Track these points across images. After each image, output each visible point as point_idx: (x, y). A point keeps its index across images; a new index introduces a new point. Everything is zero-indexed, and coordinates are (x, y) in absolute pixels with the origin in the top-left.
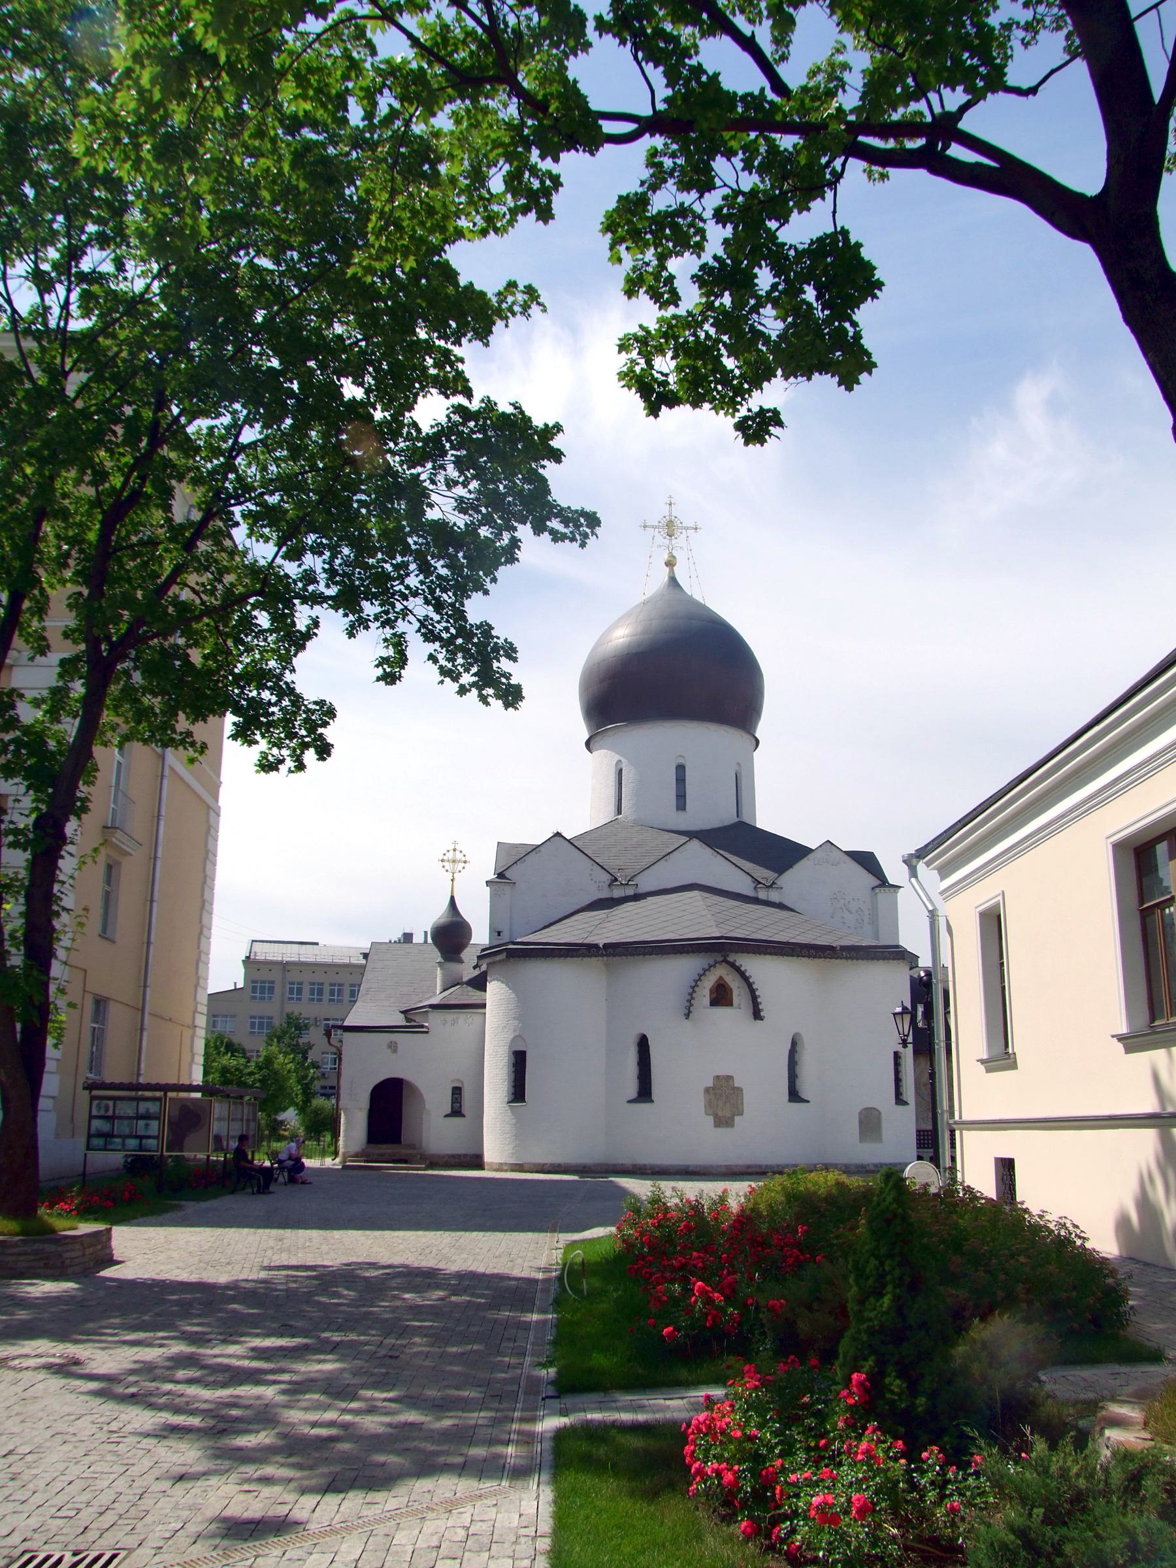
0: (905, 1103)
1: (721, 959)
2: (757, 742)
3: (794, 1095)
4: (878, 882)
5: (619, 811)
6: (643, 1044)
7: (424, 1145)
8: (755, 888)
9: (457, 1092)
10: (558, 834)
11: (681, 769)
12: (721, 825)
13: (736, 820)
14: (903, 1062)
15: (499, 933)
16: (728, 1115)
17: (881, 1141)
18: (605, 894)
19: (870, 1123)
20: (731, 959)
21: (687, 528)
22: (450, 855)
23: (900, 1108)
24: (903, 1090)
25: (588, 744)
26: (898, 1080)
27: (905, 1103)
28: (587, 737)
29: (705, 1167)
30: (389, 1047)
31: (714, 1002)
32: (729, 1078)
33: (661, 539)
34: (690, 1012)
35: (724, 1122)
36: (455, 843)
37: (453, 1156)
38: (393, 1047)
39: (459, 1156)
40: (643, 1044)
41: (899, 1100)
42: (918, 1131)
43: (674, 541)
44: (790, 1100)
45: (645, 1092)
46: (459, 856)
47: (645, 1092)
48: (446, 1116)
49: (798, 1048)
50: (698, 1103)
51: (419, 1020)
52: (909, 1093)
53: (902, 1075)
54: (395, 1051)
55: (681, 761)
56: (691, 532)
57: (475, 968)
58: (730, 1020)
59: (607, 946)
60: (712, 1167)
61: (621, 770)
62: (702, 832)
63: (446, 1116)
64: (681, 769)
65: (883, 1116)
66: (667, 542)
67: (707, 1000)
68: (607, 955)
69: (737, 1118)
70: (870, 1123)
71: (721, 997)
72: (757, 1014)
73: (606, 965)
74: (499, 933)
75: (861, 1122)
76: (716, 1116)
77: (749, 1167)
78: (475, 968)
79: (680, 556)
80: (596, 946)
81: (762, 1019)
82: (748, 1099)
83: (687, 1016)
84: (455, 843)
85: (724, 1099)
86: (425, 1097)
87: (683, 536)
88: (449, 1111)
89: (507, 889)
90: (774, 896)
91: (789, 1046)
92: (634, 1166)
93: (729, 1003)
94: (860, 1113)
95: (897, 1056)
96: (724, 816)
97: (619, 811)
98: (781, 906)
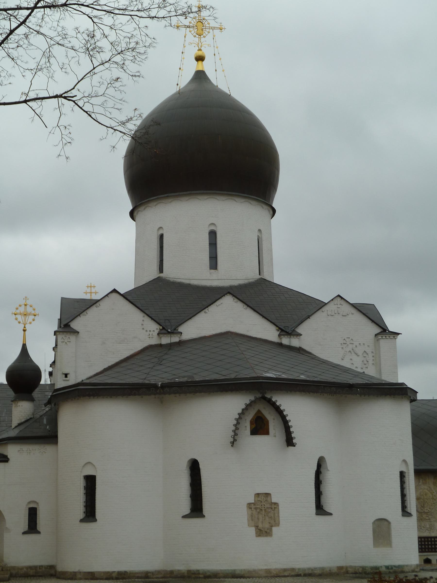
0: (410, 515)
1: (260, 396)
2: (274, 211)
3: (320, 509)
4: (378, 330)
5: (161, 270)
6: (194, 467)
7: (5, 559)
8: (279, 335)
9: (33, 513)
10: (115, 291)
11: (213, 235)
12: (246, 282)
13: (258, 277)
14: (406, 479)
15: (66, 375)
16: (267, 526)
17: (391, 546)
18: (154, 341)
19: (382, 530)
20: (268, 396)
21: (213, 28)
22: (22, 309)
23: (406, 519)
24: (408, 504)
25: (132, 214)
26: (403, 496)
27: (410, 515)
28: (131, 208)
29: (249, 572)
31: (254, 432)
32: (268, 495)
33: (191, 38)
34: (235, 440)
35: (263, 532)
37: (30, 568)
39: (35, 567)
40: (194, 467)
41: (405, 512)
42: (419, 538)
43: (203, 39)
44: (317, 514)
45: (197, 508)
46: (29, 310)
47: (197, 508)
48: (24, 533)
49: (322, 470)
50: (243, 515)
52: (412, 507)
53: (407, 491)
55: (212, 228)
56: (217, 32)
57: (46, 405)
58: (266, 445)
59: (164, 386)
60: (254, 571)
61: (161, 237)
62: (231, 287)
63: (24, 533)
64: (213, 235)
65: (393, 526)
66: (197, 39)
67: (248, 431)
68: (165, 393)
69: (274, 529)
70: (382, 530)
71: (259, 427)
72: (290, 441)
73: (162, 402)
74: (66, 375)
75: (374, 531)
76: (257, 527)
77: (285, 570)
78: (46, 405)
79: (207, 52)
80: (155, 386)
81: (293, 445)
82: (284, 513)
83: (233, 443)
85: (264, 513)
86: (6, 518)
87: (210, 36)
88: (26, 528)
89: (73, 338)
90: (295, 342)
91: (315, 468)
92: (189, 571)
93: (267, 433)
94: (374, 523)
95: (402, 475)
96: (249, 274)
97: (161, 270)
98: (300, 350)
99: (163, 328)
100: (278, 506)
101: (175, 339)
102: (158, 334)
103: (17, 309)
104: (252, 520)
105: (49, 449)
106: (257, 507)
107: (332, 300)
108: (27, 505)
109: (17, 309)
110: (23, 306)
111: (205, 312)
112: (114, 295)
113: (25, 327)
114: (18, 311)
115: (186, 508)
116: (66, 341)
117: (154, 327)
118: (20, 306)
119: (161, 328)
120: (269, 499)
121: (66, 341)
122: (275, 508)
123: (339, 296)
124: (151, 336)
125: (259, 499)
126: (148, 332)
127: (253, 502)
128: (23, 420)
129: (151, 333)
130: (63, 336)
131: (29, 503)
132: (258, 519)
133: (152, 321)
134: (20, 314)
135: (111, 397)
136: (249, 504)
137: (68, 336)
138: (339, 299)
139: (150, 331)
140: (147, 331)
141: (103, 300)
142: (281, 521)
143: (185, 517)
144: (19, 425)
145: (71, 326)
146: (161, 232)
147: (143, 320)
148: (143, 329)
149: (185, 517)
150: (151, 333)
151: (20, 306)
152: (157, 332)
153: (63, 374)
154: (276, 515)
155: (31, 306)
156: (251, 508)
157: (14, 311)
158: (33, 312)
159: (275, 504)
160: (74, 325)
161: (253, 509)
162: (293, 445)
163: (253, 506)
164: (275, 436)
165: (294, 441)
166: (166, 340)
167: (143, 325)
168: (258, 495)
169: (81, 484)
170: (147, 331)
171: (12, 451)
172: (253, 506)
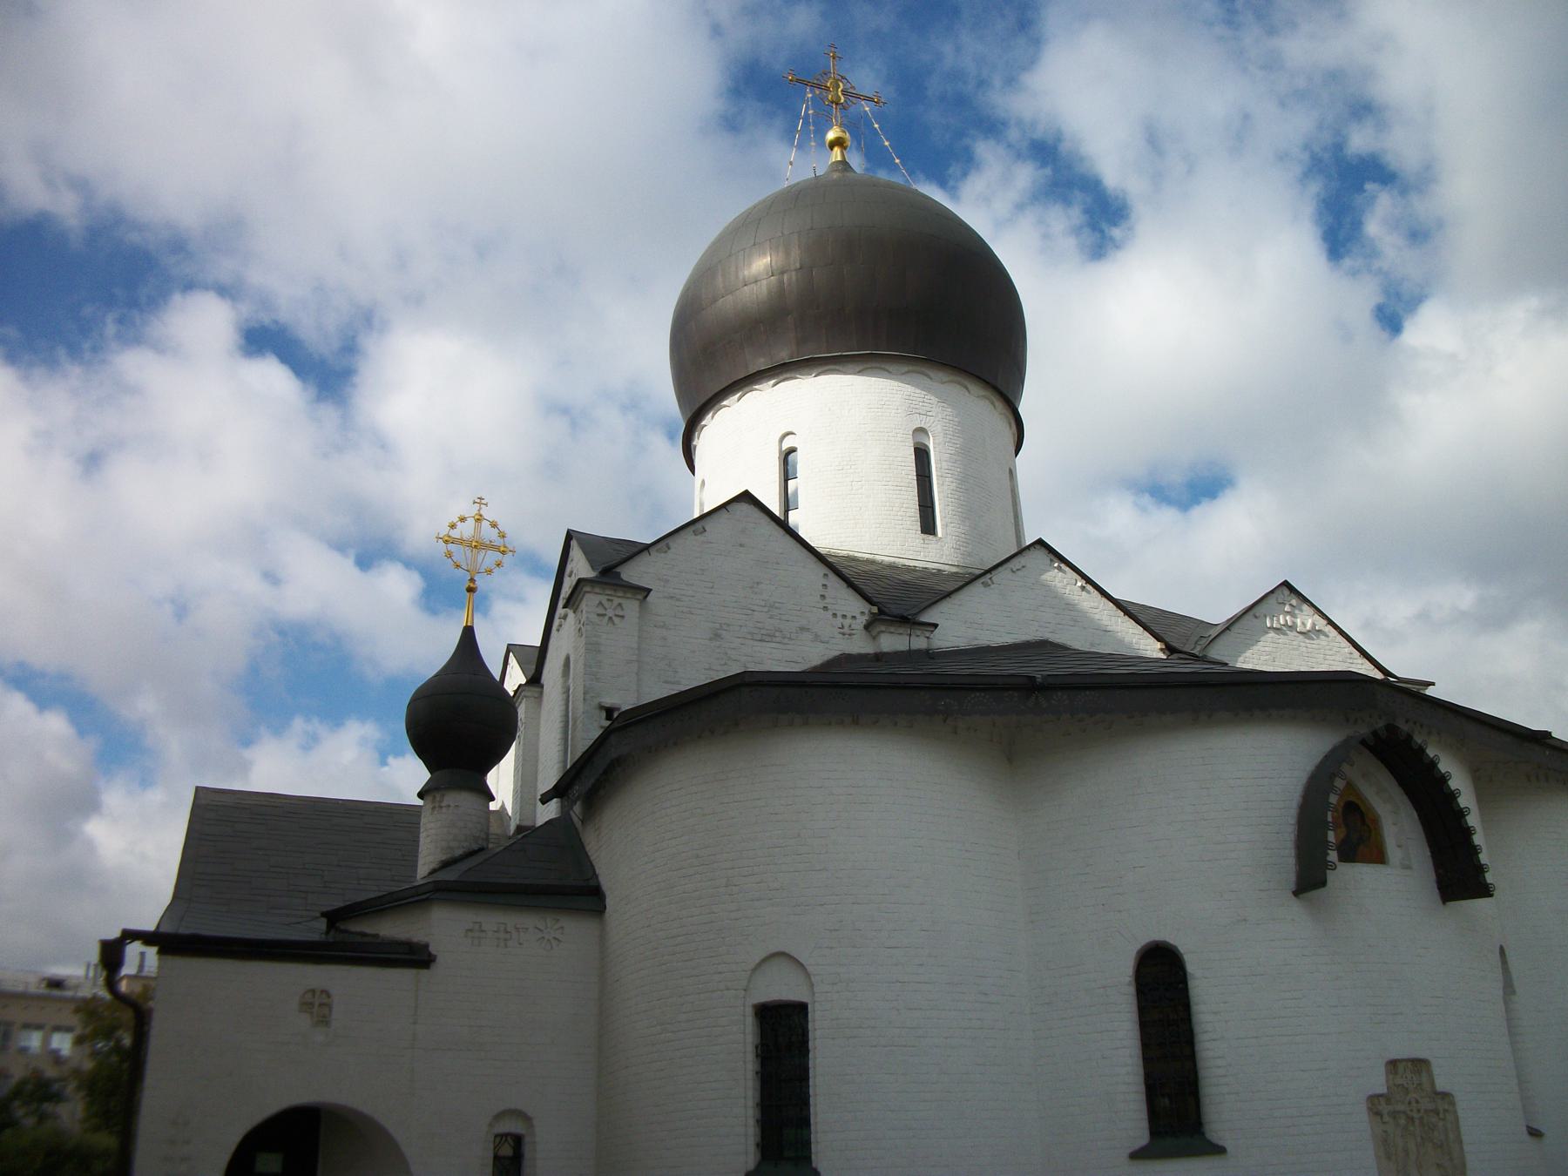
6: (1161, 978)
18: (860, 645)
22: (466, 530)
30: (306, 1006)
31: (1350, 854)
36: (480, 501)
38: (318, 1006)
40: (1161, 978)
46: (489, 534)
51: (391, 928)
54: (324, 1021)
73: (1010, 760)
78: (545, 799)
84: (480, 501)
89: (631, 606)
93: (1379, 857)
99: (881, 612)
100: (1453, 1104)
101: (919, 643)
102: (867, 627)
103: (453, 526)
104: (1389, 1158)
105: (572, 932)
106: (1401, 1107)
107: (1272, 592)
108: (490, 1125)
109: (453, 526)
110: (471, 522)
111: (986, 585)
112: (745, 508)
113: (472, 580)
114: (455, 534)
115: (1133, 1124)
116: (610, 613)
117: (855, 608)
118: (463, 519)
119: (875, 610)
120: (1424, 1079)
121: (610, 613)
122: (1446, 1111)
123: (1286, 584)
124: (846, 630)
125: (1399, 1081)
126: (840, 618)
127: (1383, 1090)
128: (458, 852)
129: (847, 622)
130: (603, 598)
131: (499, 1117)
132: (1406, 1151)
133: (850, 591)
134: (460, 541)
135: (856, 722)
136: (1373, 1100)
137: (617, 601)
138: (1287, 592)
139: (844, 616)
140: (835, 615)
141: (714, 516)
142: (1468, 1157)
143: (1137, 1155)
144: (445, 865)
145: (624, 576)
146: (786, 445)
147: (825, 586)
148: (825, 608)
149: (1137, 1155)
150: (847, 622)
151: (463, 519)
152: (863, 620)
153: (602, 707)
154: (1451, 1136)
155: (494, 525)
156: (1378, 1114)
157: (444, 531)
158: (498, 542)
159: (1446, 1096)
160: (631, 573)
161: (1386, 1118)
162: (1485, 891)
163: (1385, 1108)
164: (1408, 867)
165: (1489, 878)
166: (892, 641)
167: (823, 597)
168: (1393, 1065)
169: (743, 1036)
170: (835, 615)
171: (442, 928)
172: (1385, 1108)
